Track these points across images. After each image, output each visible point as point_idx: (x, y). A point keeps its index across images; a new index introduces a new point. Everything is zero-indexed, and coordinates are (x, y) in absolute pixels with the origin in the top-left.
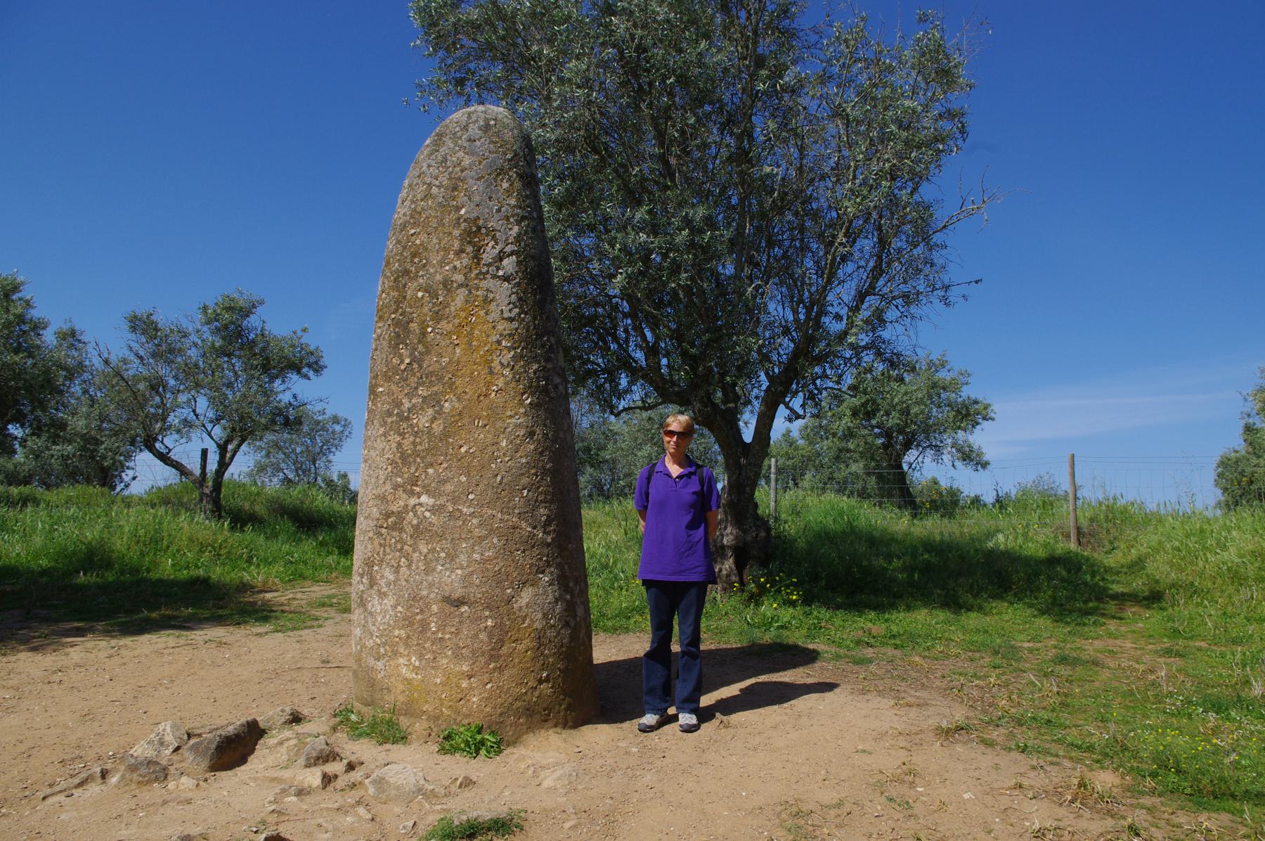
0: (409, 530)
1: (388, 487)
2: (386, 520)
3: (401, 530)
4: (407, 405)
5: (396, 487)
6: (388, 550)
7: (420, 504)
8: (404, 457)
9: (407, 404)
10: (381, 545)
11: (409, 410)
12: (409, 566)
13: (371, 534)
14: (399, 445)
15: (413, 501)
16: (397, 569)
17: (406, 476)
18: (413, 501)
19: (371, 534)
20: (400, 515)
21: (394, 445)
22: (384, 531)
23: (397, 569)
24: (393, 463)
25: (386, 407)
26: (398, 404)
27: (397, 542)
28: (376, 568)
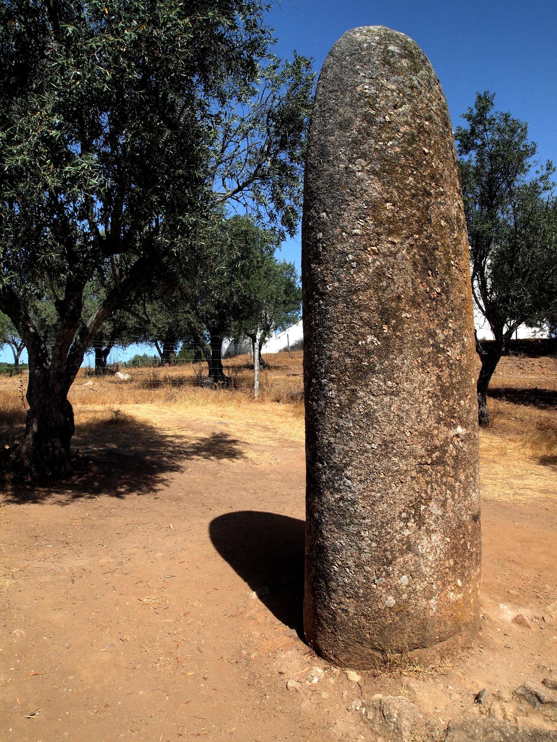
0: (451, 462)
1: (432, 422)
2: (430, 456)
3: (444, 463)
4: (441, 337)
5: (439, 420)
6: (435, 486)
7: (457, 436)
8: (443, 389)
9: (441, 337)
10: (428, 483)
11: (444, 341)
12: (453, 497)
13: (414, 474)
14: (439, 378)
15: (452, 433)
16: (444, 504)
17: (446, 409)
18: (452, 433)
19: (414, 474)
20: (443, 449)
21: (434, 378)
22: (426, 467)
23: (444, 504)
24: (433, 396)
25: (418, 336)
26: (433, 335)
27: (442, 476)
28: (423, 507)
